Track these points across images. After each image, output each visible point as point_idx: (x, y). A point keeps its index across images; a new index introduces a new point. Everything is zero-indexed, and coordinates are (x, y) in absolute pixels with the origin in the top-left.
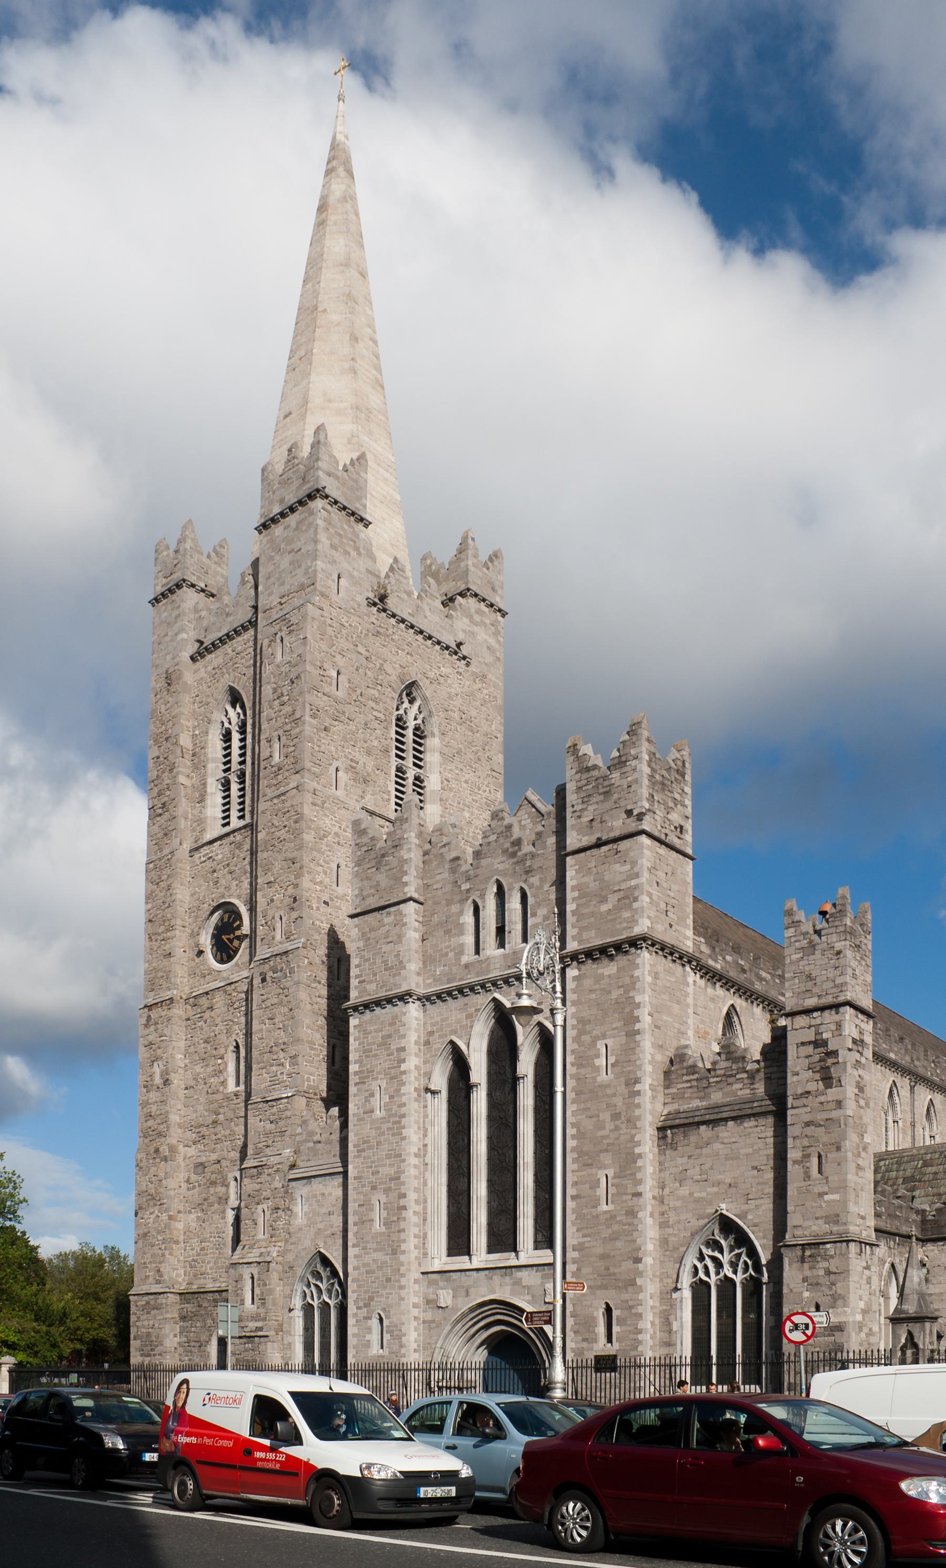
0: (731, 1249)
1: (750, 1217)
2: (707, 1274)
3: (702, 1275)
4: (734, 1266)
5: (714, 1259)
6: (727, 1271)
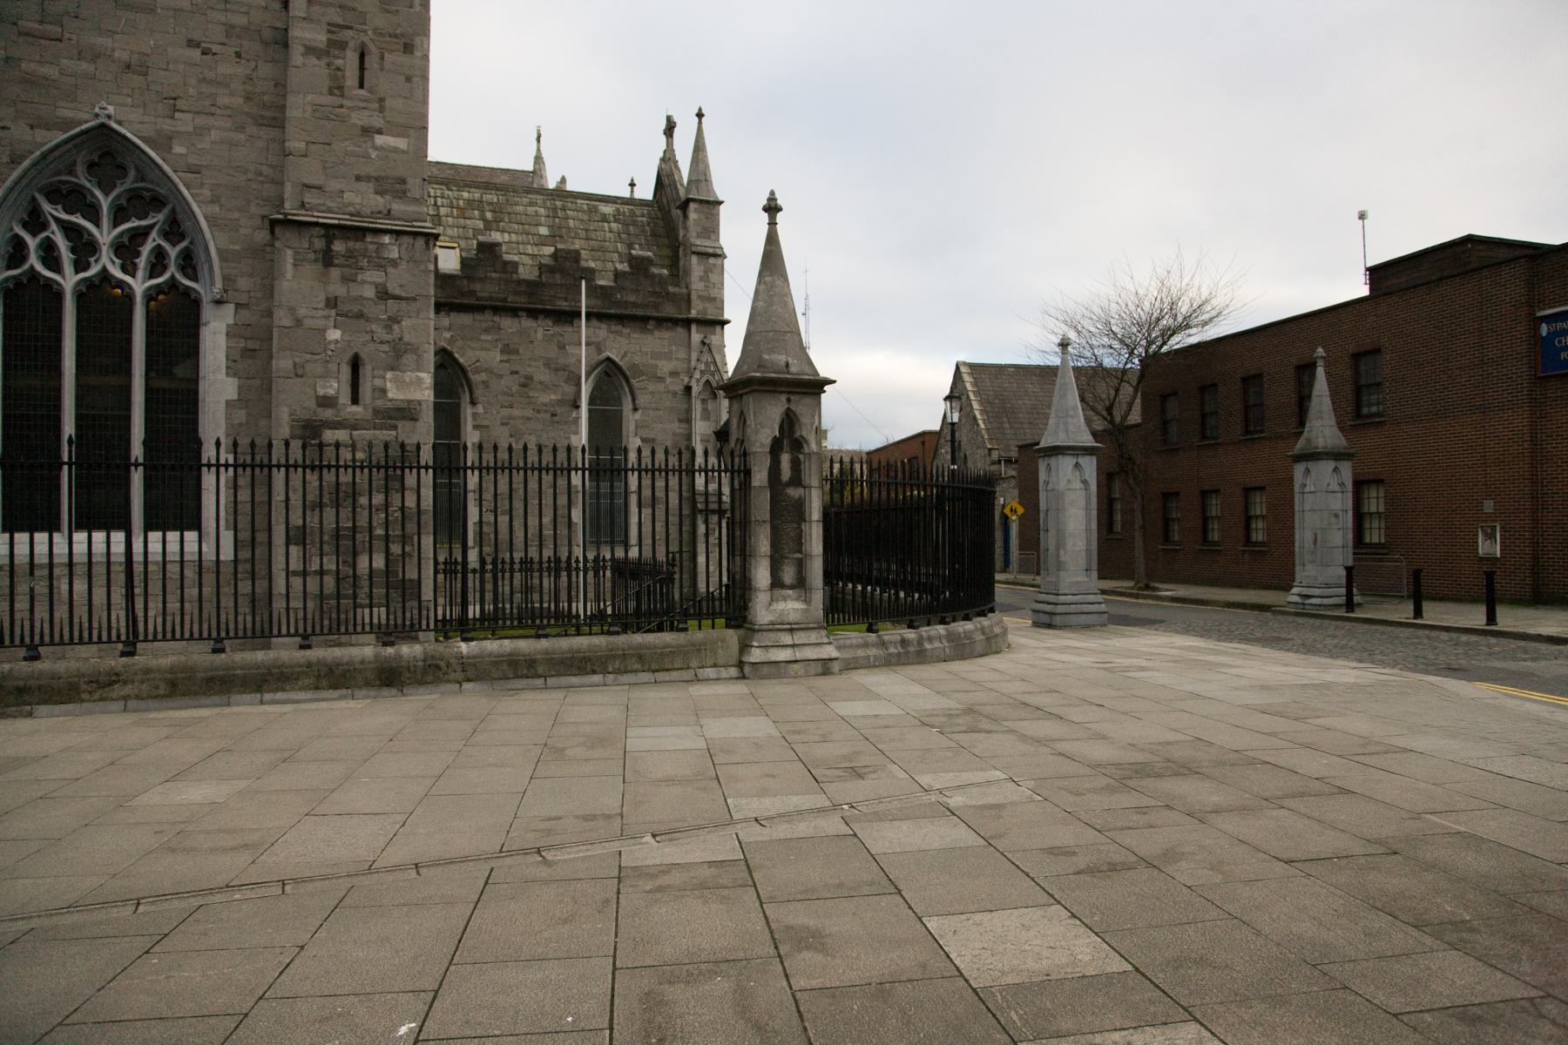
0: (119, 216)
1: (178, 149)
2: (54, 264)
3: (34, 261)
4: (126, 250)
5: (70, 230)
6: (107, 261)
